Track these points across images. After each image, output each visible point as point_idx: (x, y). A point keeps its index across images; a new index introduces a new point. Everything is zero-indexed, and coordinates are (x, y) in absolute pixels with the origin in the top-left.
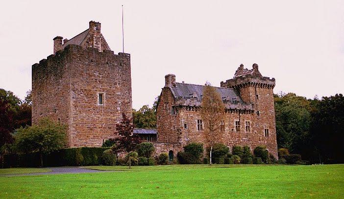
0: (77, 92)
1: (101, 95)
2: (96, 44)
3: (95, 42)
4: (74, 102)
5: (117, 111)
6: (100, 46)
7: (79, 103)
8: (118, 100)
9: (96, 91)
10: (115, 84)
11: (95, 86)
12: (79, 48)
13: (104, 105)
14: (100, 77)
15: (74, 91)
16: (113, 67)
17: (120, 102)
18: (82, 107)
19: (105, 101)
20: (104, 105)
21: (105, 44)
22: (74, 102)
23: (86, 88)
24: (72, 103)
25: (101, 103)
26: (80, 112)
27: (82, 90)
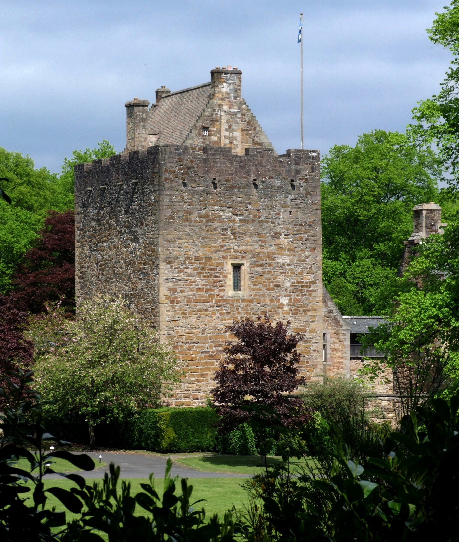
0: (175, 265)
1: (237, 268)
2: (226, 130)
3: (225, 126)
4: (170, 290)
5: (280, 307)
6: (237, 134)
7: (182, 292)
8: (282, 277)
9: (224, 258)
10: (276, 235)
11: (222, 247)
12: (180, 151)
13: (244, 293)
14: (234, 221)
15: (169, 263)
16: (270, 193)
17: (288, 284)
18: (189, 302)
19: (246, 280)
20: (244, 293)
21: (251, 126)
22: (170, 290)
23: (200, 254)
24: (164, 292)
25: (237, 286)
26: (184, 314)
27: (188, 258)
